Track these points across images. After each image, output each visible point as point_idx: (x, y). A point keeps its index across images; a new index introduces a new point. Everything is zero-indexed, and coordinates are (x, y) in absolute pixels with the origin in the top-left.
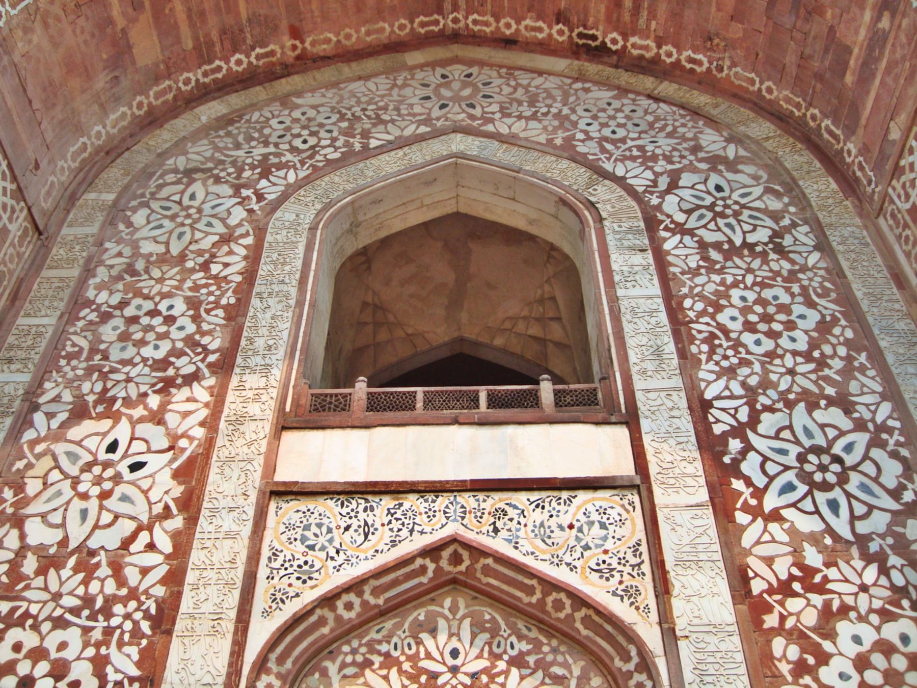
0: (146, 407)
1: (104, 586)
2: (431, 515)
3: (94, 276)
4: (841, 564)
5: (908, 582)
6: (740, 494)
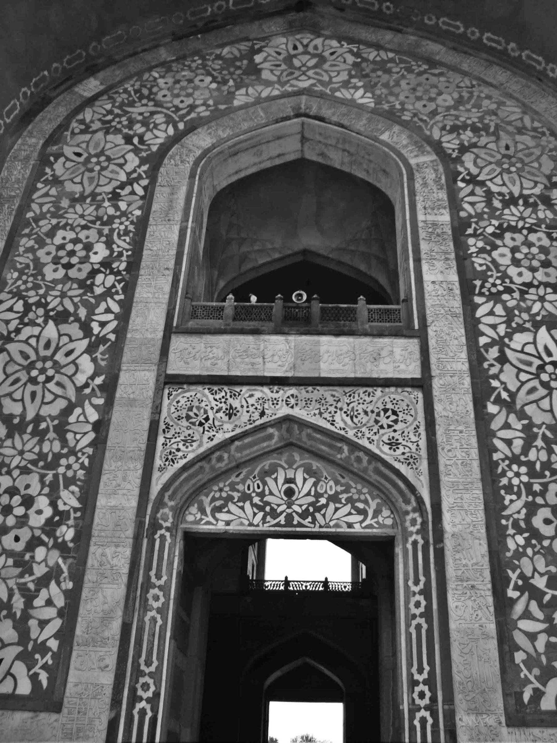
1: (52, 446)
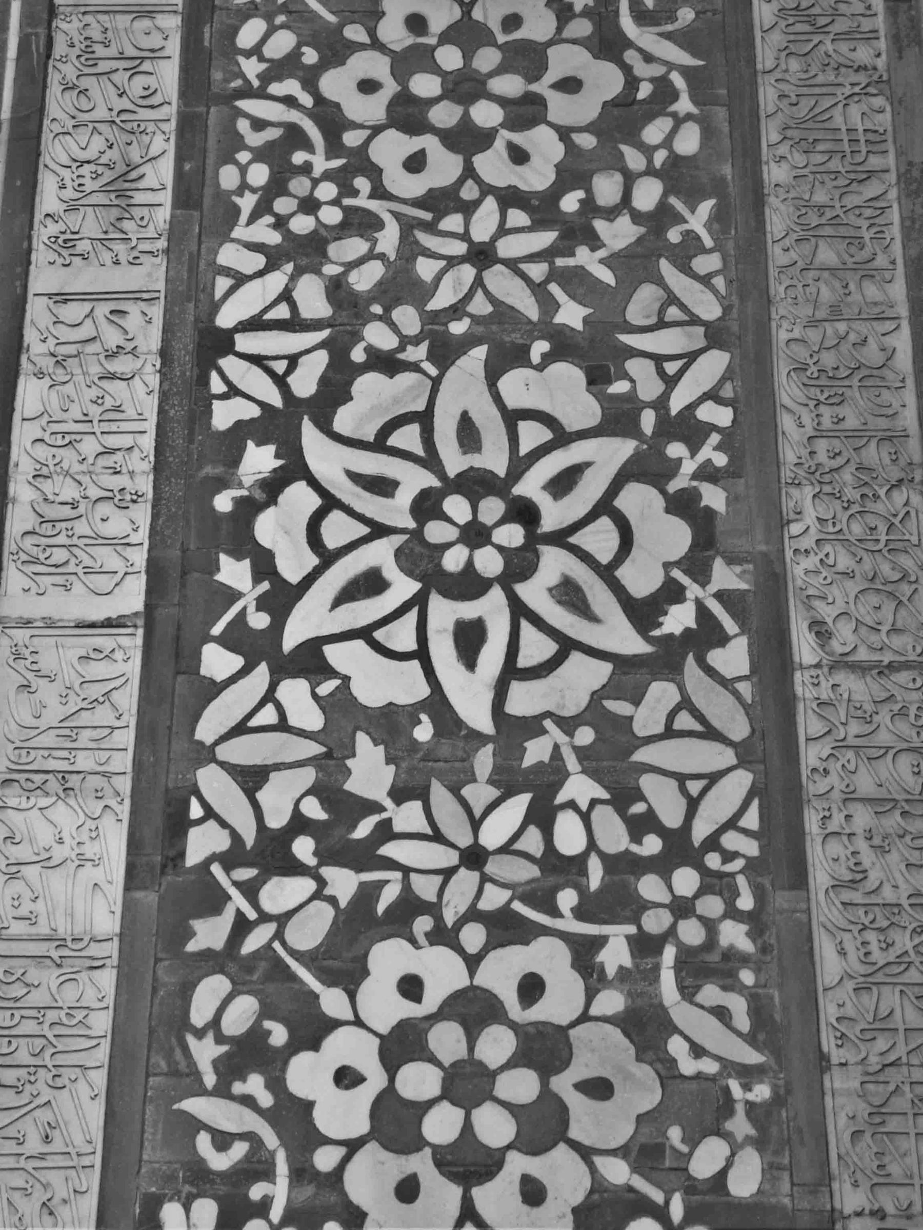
4: (439, 793)
5: (592, 844)
6: (233, 595)
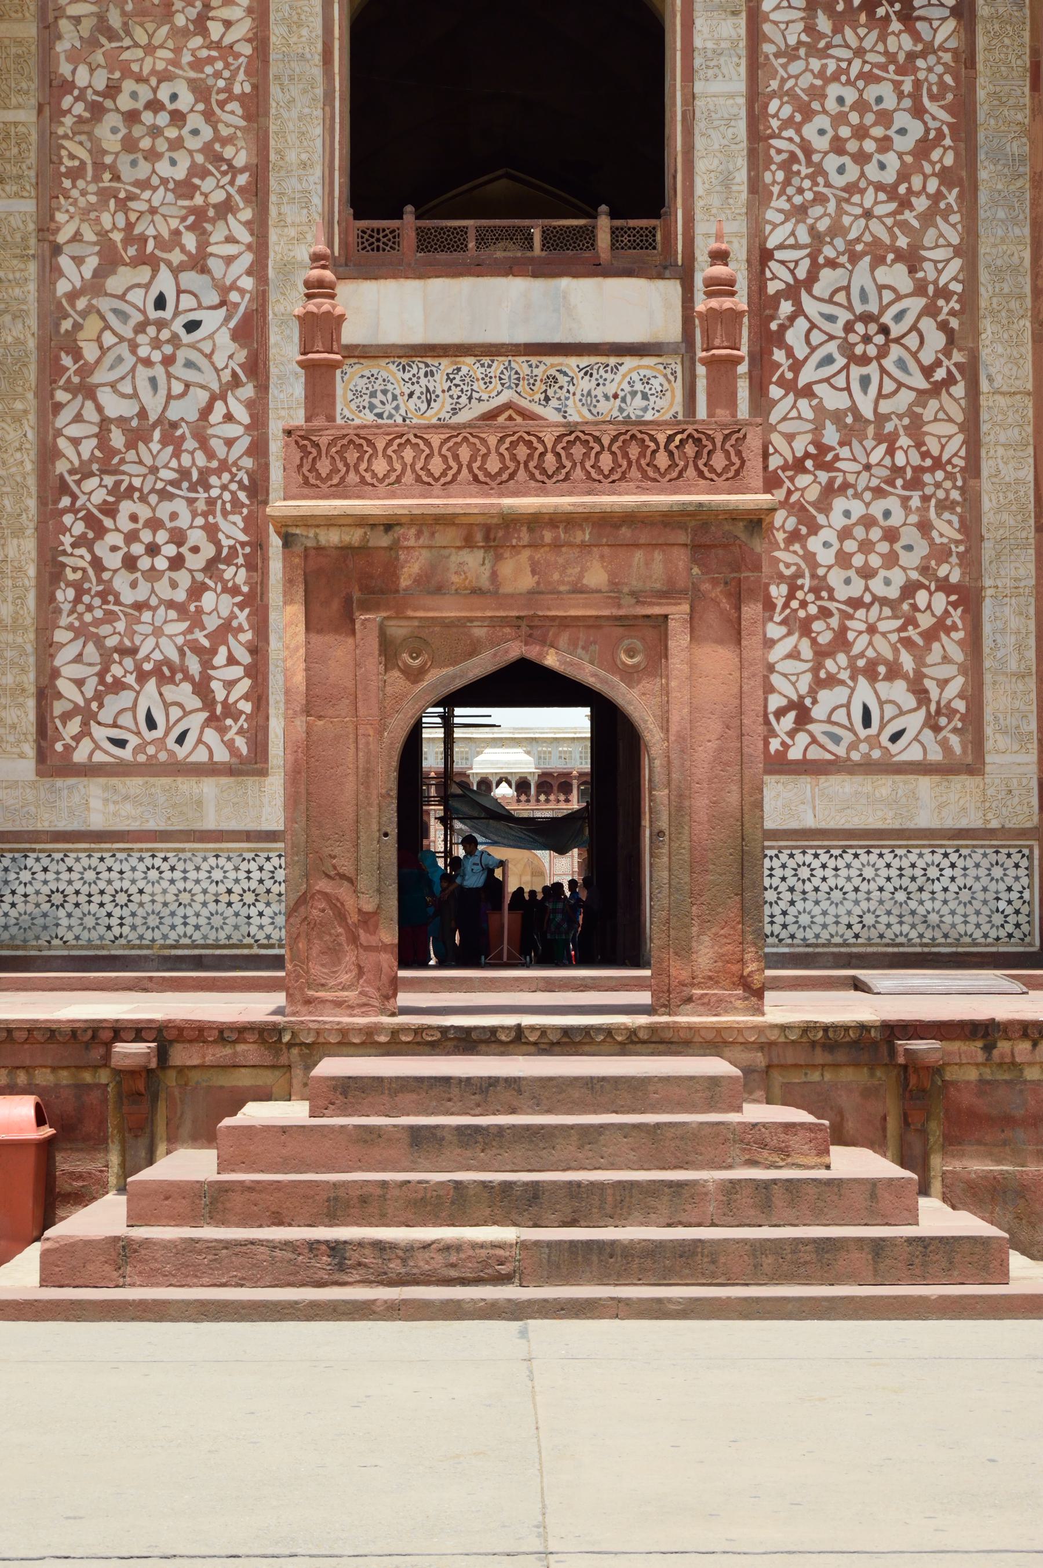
0: (183, 250)
2: (487, 381)
3: (59, 37)
